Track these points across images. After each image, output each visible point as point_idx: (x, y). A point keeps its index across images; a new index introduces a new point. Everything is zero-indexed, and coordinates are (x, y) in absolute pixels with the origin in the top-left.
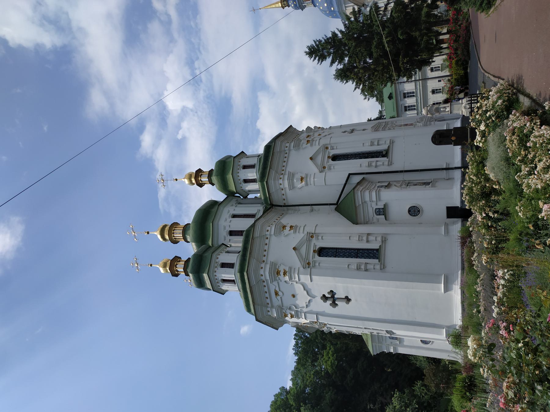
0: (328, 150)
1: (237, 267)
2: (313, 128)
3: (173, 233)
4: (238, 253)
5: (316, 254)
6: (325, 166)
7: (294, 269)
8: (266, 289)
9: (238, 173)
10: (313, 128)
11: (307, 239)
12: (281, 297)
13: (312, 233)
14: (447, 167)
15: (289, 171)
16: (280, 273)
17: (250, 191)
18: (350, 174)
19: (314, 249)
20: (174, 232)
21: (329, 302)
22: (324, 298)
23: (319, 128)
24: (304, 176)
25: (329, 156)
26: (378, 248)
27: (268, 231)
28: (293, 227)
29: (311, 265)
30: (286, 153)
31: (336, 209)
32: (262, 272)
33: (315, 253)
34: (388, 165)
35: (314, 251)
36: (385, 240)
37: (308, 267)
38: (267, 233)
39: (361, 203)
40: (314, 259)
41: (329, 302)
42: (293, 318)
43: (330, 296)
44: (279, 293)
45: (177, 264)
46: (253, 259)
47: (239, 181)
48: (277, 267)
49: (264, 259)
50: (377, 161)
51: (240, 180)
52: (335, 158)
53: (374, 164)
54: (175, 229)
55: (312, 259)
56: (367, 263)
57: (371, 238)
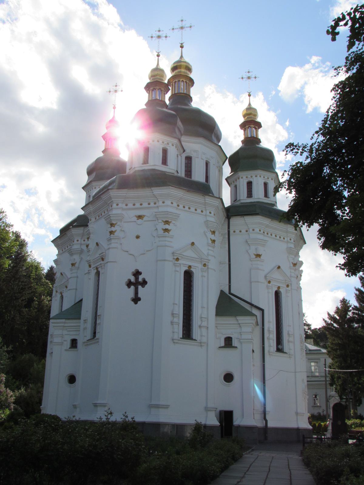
0: (285, 286)
1: (163, 168)
2: (301, 269)
3: (183, 81)
4: (177, 171)
5: (187, 268)
6: (271, 283)
7: (171, 242)
8: (145, 205)
9: (260, 177)
10: (301, 269)
11: (203, 259)
12: (136, 222)
13: (208, 265)
14: (267, 413)
15: (268, 241)
16: (167, 225)
17: (236, 186)
18: (262, 310)
19: (192, 267)
20: (184, 82)
21: (133, 279)
22: (137, 273)
24: (261, 257)
25: (281, 287)
26: (194, 338)
27: (210, 213)
28: (214, 244)
29: (176, 262)
30: (284, 238)
31: (222, 292)
32: (168, 202)
33: (188, 267)
34: (269, 352)
35: (190, 267)
36: (201, 346)
37: (174, 258)
38: (208, 212)
39: (240, 322)
40: (182, 265)
41: (133, 279)
42: (109, 234)
43: (140, 279)
44: (140, 220)
45: (162, 91)
46: (183, 194)
47: (249, 176)
48: (173, 222)
49: (181, 207)
50: (273, 340)
51: (252, 177)
52: (277, 295)
54: (188, 84)
55: (182, 264)
56: (179, 325)
57: (204, 330)
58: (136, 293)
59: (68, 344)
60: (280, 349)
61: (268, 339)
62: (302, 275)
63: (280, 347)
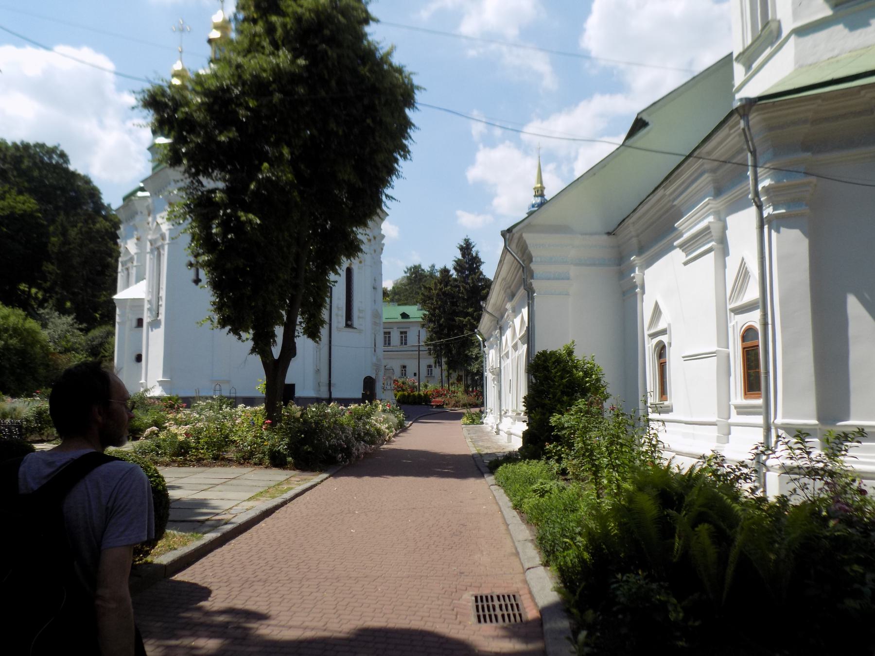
23: (382, 249)
53: (340, 313)
58: (197, 274)
59: (134, 323)
60: (349, 324)
61: (337, 315)
62: (384, 248)
63: (349, 323)
